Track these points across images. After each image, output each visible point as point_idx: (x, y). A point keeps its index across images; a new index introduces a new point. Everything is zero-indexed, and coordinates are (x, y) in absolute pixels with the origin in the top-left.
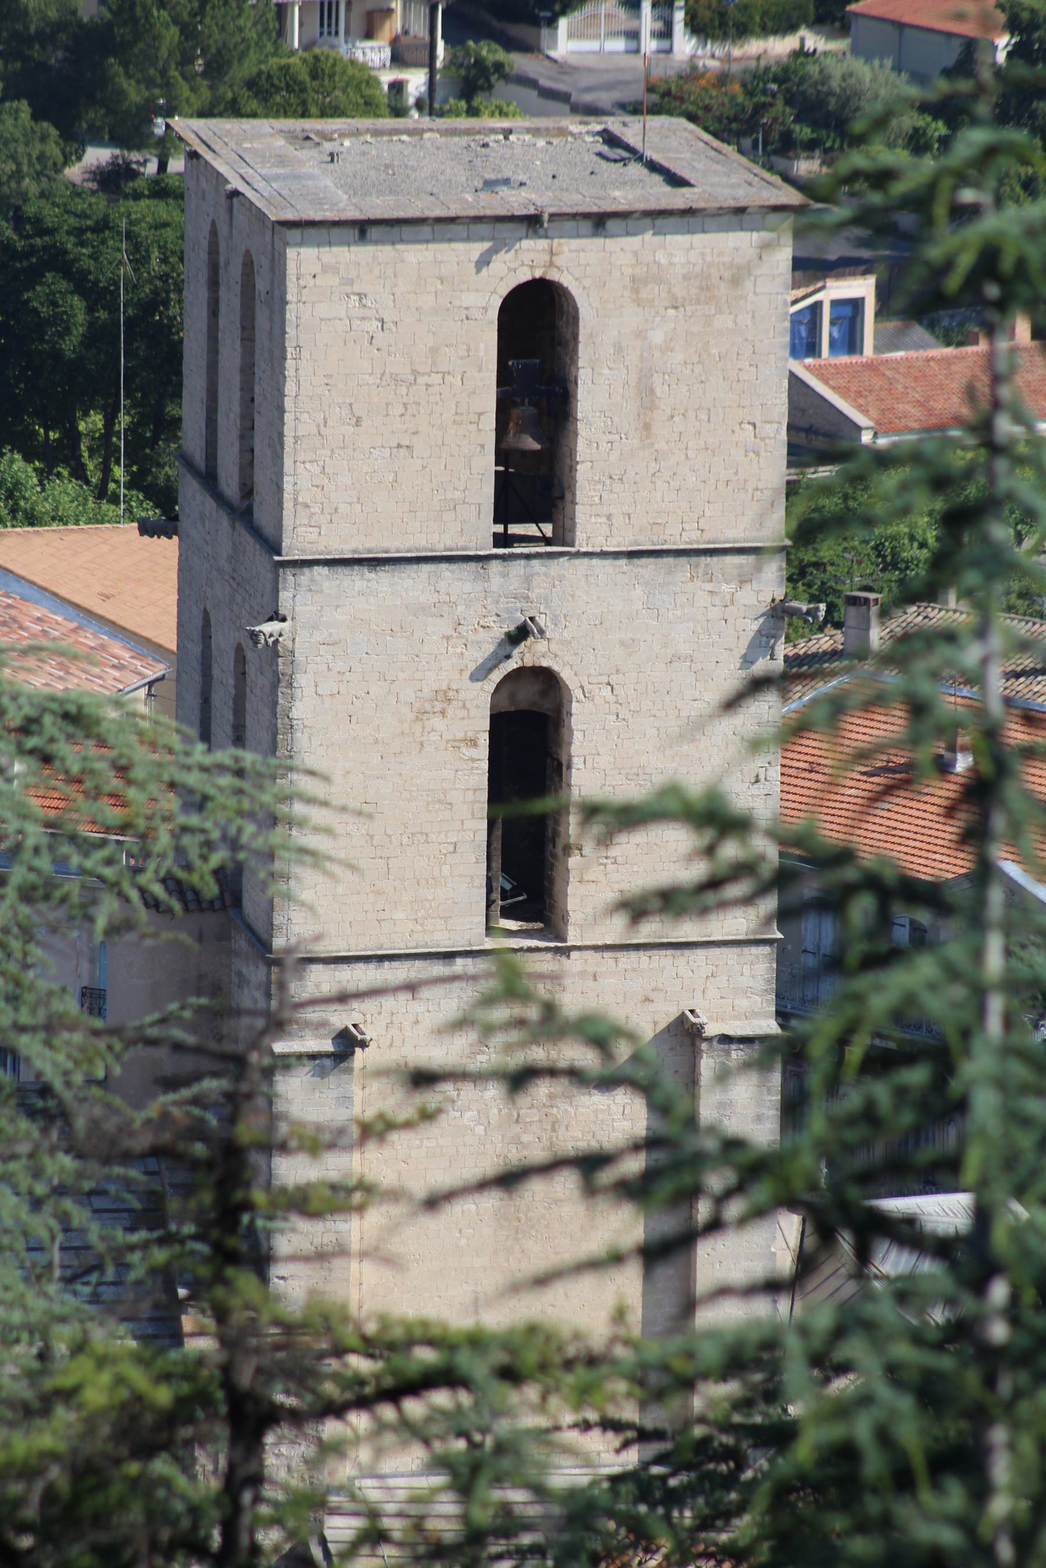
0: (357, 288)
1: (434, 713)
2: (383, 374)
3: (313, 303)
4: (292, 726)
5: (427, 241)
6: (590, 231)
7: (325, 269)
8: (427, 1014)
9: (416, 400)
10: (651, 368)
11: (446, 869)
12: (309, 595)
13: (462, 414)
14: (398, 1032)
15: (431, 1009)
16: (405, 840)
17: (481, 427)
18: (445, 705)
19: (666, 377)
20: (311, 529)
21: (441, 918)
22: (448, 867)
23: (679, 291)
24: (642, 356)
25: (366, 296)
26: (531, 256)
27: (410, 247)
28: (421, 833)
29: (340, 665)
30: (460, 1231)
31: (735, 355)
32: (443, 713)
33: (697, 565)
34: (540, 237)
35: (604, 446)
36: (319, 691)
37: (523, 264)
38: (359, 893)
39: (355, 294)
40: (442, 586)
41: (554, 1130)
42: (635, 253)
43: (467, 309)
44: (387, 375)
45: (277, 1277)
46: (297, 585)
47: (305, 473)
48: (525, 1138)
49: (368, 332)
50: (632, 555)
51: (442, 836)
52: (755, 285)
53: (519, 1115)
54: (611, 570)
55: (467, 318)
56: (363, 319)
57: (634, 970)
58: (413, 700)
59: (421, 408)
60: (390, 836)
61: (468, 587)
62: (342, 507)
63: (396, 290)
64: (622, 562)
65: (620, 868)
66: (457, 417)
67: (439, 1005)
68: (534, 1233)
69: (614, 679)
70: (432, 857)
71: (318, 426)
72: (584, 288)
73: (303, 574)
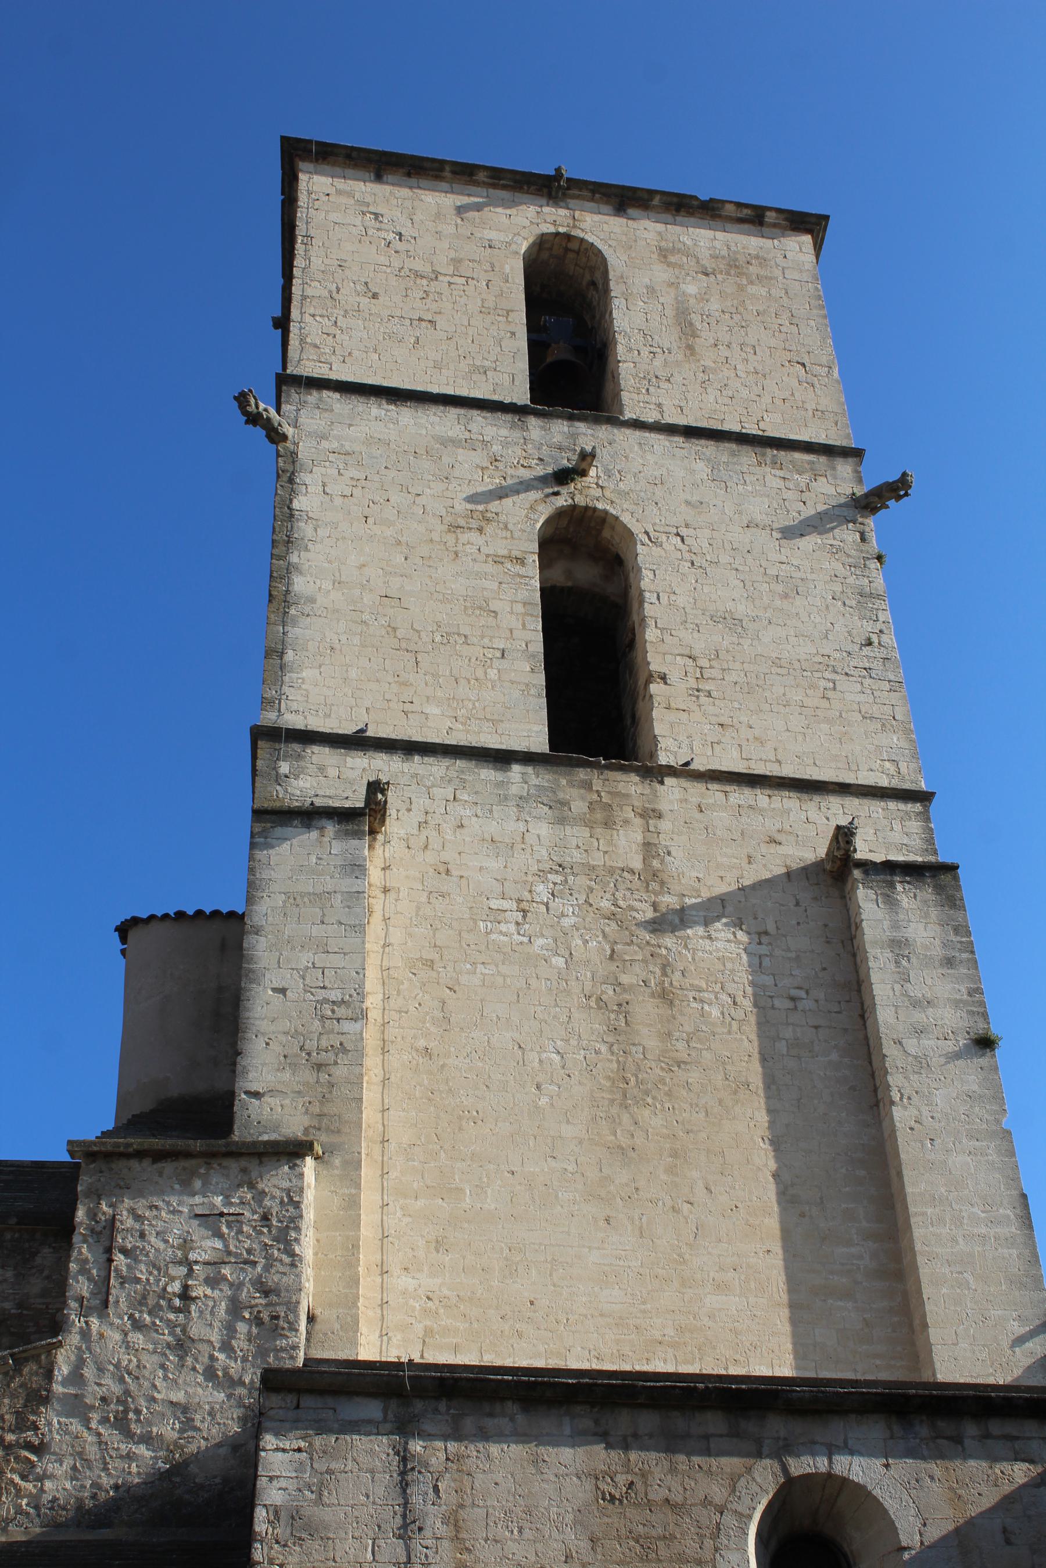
0: (372, 209)
1: (471, 529)
2: (402, 268)
3: (327, 212)
4: (292, 516)
5: (446, 192)
6: (611, 212)
7: (339, 192)
8: (474, 819)
9: (438, 290)
10: (688, 309)
11: (493, 674)
12: (317, 411)
13: (489, 308)
14: (434, 833)
15: (480, 814)
16: (438, 639)
17: (510, 319)
18: (483, 524)
19: (704, 317)
20: (321, 365)
21: (488, 720)
22: (496, 671)
23: (709, 264)
24: (676, 299)
25: (382, 216)
26: (554, 218)
27: (427, 192)
28: (459, 634)
29: (353, 473)
30: (538, 1087)
31: (774, 315)
32: (480, 530)
33: (764, 455)
34: (561, 207)
35: (645, 352)
36: (327, 490)
37: (545, 222)
38: (378, 681)
39: (371, 213)
40: (474, 427)
41: (664, 974)
42: (660, 233)
43: (489, 240)
44: (406, 270)
45: (246, 1093)
46: (303, 404)
47: (316, 323)
48: (625, 979)
49: (385, 239)
50: (691, 432)
51: (486, 641)
52: (784, 273)
53: (613, 951)
54: (667, 443)
55: (490, 247)
56: (378, 229)
57: (750, 807)
58: (444, 514)
59: (443, 296)
60: (417, 631)
61: (504, 432)
62: (356, 353)
63: (415, 217)
64: (679, 440)
65: (717, 702)
66: (483, 309)
67: (491, 811)
68: (649, 1100)
69: (683, 532)
70: (473, 660)
71: (330, 292)
72: (610, 246)
73: (311, 394)
